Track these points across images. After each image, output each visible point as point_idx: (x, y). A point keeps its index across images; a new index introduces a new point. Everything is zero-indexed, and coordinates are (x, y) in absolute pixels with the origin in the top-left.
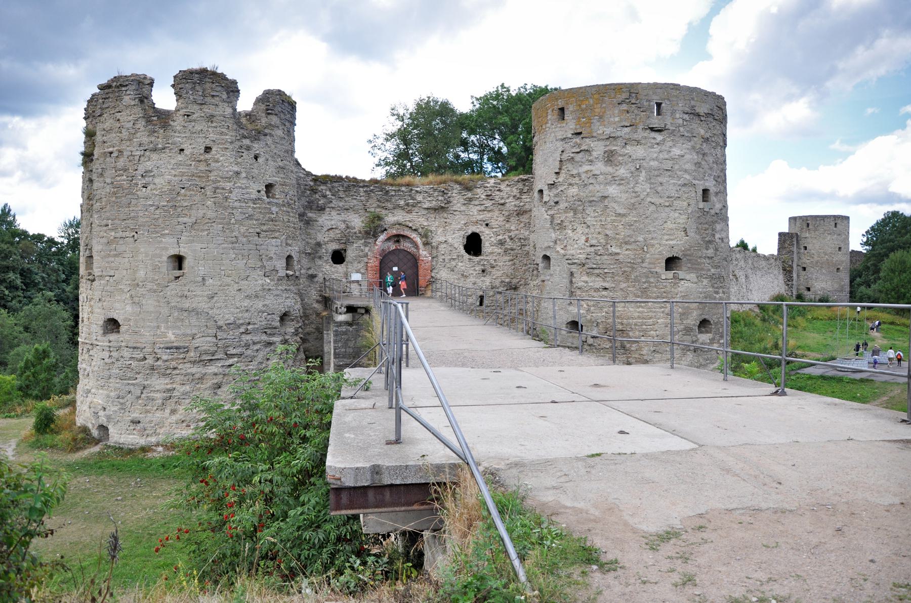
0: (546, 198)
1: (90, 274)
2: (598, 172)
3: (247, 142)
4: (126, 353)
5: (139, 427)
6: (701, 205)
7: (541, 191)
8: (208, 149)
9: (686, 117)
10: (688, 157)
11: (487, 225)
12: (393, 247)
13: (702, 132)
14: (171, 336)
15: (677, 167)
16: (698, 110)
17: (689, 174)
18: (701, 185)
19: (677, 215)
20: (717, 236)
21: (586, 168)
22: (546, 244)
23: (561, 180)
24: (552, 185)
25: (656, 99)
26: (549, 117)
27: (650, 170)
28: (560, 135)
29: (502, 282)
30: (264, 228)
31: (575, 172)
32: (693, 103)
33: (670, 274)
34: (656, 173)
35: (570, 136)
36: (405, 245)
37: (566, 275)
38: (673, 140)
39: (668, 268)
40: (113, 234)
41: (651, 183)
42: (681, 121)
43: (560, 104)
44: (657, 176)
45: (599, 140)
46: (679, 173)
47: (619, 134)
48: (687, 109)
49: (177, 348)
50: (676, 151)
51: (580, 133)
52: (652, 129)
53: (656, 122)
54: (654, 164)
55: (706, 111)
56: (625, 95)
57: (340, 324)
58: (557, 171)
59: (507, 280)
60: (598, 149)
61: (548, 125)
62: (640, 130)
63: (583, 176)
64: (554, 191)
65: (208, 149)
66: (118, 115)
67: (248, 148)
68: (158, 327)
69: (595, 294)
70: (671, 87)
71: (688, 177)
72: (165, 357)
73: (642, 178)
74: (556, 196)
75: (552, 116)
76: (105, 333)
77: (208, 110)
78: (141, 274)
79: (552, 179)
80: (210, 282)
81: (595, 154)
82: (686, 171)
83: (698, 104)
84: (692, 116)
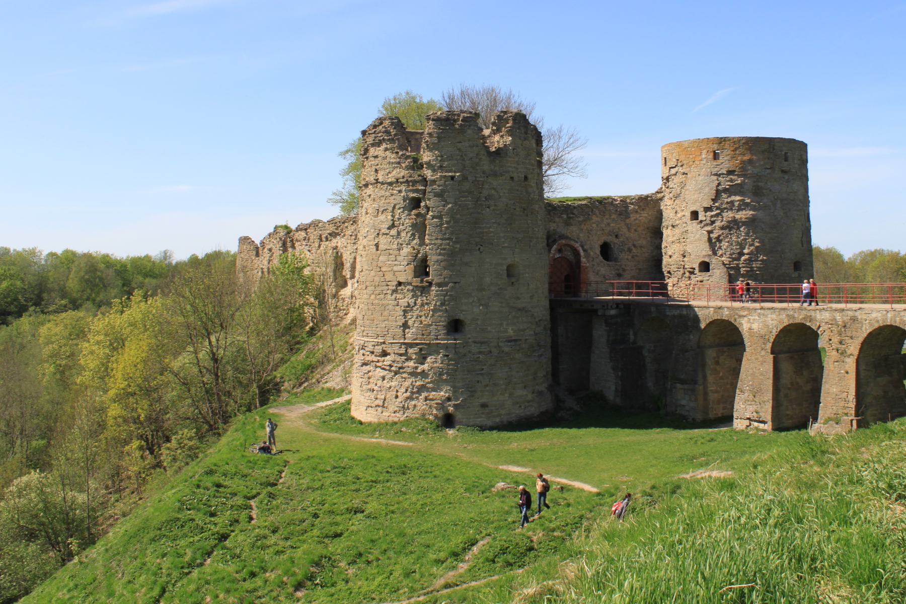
0: (701, 217)
1: (422, 281)
4: (474, 348)
5: (487, 410)
8: (526, 178)
12: (557, 256)
14: (510, 332)
21: (738, 198)
22: (704, 253)
24: (707, 209)
26: (704, 156)
28: (715, 171)
31: (729, 200)
36: (569, 255)
37: (726, 277)
40: (458, 246)
49: (515, 341)
52: (783, 171)
56: (766, 146)
57: (612, 317)
63: (736, 204)
65: (526, 178)
66: (459, 145)
68: (501, 324)
72: (507, 349)
74: (712, 216)
76: (448, 334)
78: (487, 280)
81: (746, 187)
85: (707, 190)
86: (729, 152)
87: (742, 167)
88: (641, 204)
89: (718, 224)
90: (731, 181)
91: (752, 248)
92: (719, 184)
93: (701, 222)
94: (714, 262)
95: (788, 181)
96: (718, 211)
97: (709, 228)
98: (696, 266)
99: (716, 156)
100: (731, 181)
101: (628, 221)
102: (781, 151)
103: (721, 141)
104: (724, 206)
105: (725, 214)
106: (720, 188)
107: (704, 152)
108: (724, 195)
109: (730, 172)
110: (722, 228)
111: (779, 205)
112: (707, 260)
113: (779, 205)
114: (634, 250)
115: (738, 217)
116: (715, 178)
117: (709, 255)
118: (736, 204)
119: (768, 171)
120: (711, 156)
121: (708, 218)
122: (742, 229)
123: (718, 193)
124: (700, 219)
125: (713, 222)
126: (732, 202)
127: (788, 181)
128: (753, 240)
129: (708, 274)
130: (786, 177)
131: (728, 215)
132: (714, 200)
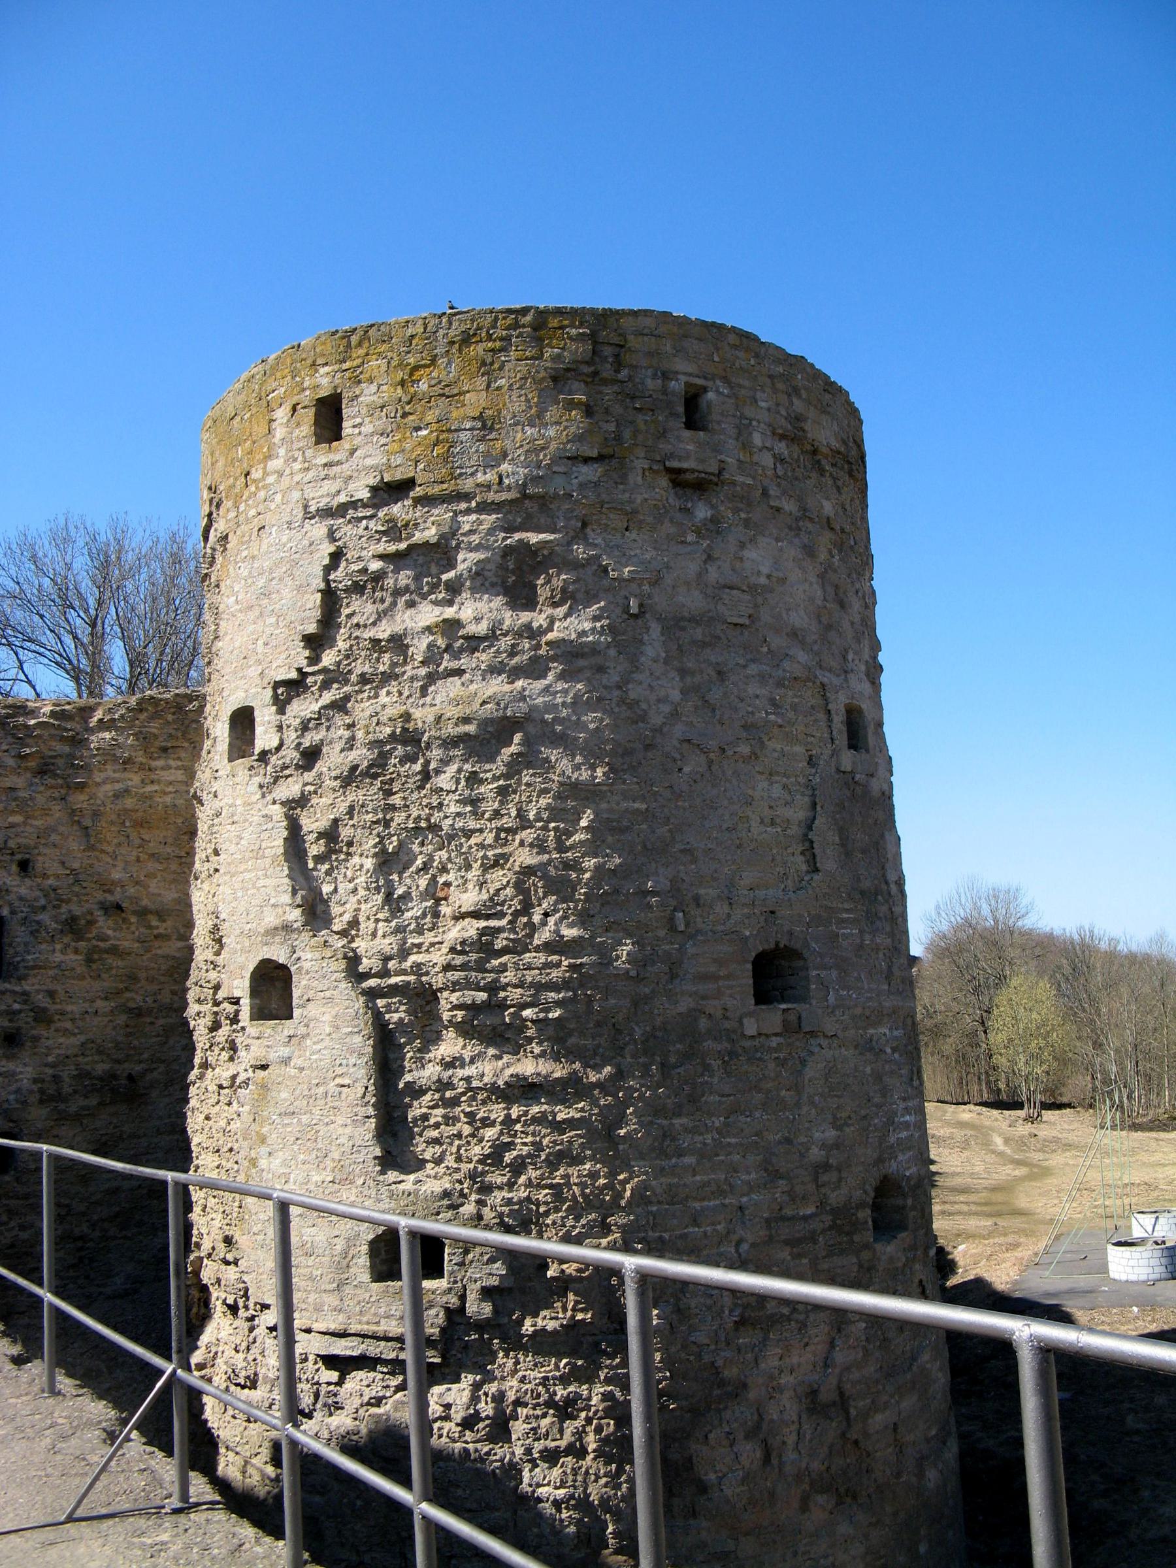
0: (265, 738)
2: (482, 628)
6: (847, 759)
7: (243, 720)
9: (782, 447)
11: (24, 866)
15: (765, 617)
19: (777, 791)
21: (429, 614)
22: (271, 919)
23: (328, 659)
24: (289, 690)
25: (685, 372)
26: (280, 432)
27: (674, 624)
28: (322, 494)
29: (83, 1075)
31: (383, 631)
32: (798, 405)
33: (773, 1017)
34: (699, 633)
35: (365, 494)
38: (747, 523)
39: (762, 997)
41: (683, 672)
42: (767, 460)
43: (324, 381)
44: (704, 645)
45: (483, 508)
46: (778, 642)
47: (558, 486)
51: (407, 485)
52: (677, 478)
53: (687, 449)
54: (693, 601)
55: (835, 444)
58: (312, 628)
59: (101, 1068)
60: (478, 538)
61: (274, 464)
62: (635, 478)
63: (419, 647)
64: (304, 707)
69: (497, 1111)
70: (732, 338)
71: (802, 657)
73: (650, 651)
75: (291, 430)
79: (289, 660)
81: (466, 561)
82: (794, 634)
83: (812, 413)
85: (287, 593)
86: (388, 393)
87: (446, 458)
88: (154, 727)
89: (333, 761)
90: (393, 530)
91: (499, 878)
92: (336, 557)
93: (264, 756)
94: (315, 970)
95: (713, 528)
96: (328, 697)
97: (291, 788)
98: (240, 987)
99: (329, 419)
100: (393, 530)
101: (79, 800)
102: (666, 376)
103: (350, 342)
104: (361, 667)
105: (362, 710)
106: (337, 574)
107: (282, 414)
108: (359, 608)
109: (390, 490)
110: (350, 778)
111: (654, 644)
112: (280, 955)
113: (654, 644)
114: (105, 925)
115: (422, 715)
116: (318, 530)
117: (286, 928)
118: (419, 647)
119: (589, 472)
120: (306, 428)
121: (291, 736)
122: (444, 781)
123: (330, 600)
124: (260, 744)
125: (311, 756)
126: (398, 643)
127: (713, 528)
128: (504, 835)
129: (287, 1027)
130: (702, 512)
131: (377, 710)
132: (316, 643)
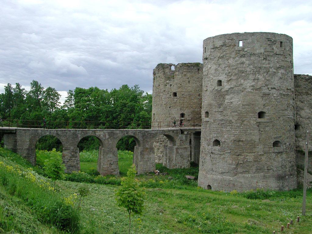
3: (168, 81)
9: (213, 50)
10: (212, 67)
13: (219, 55)
16: (216, 46)
17: (213, 75)
18: (217, 79)
20: (226, 101)
30: (171, 105)
48: (212, 47)
50: (209, 66)
55: (220, 45)
67: (168, 83)
77: (159, 74)
80: (158, 120)
84: (215, 49)
